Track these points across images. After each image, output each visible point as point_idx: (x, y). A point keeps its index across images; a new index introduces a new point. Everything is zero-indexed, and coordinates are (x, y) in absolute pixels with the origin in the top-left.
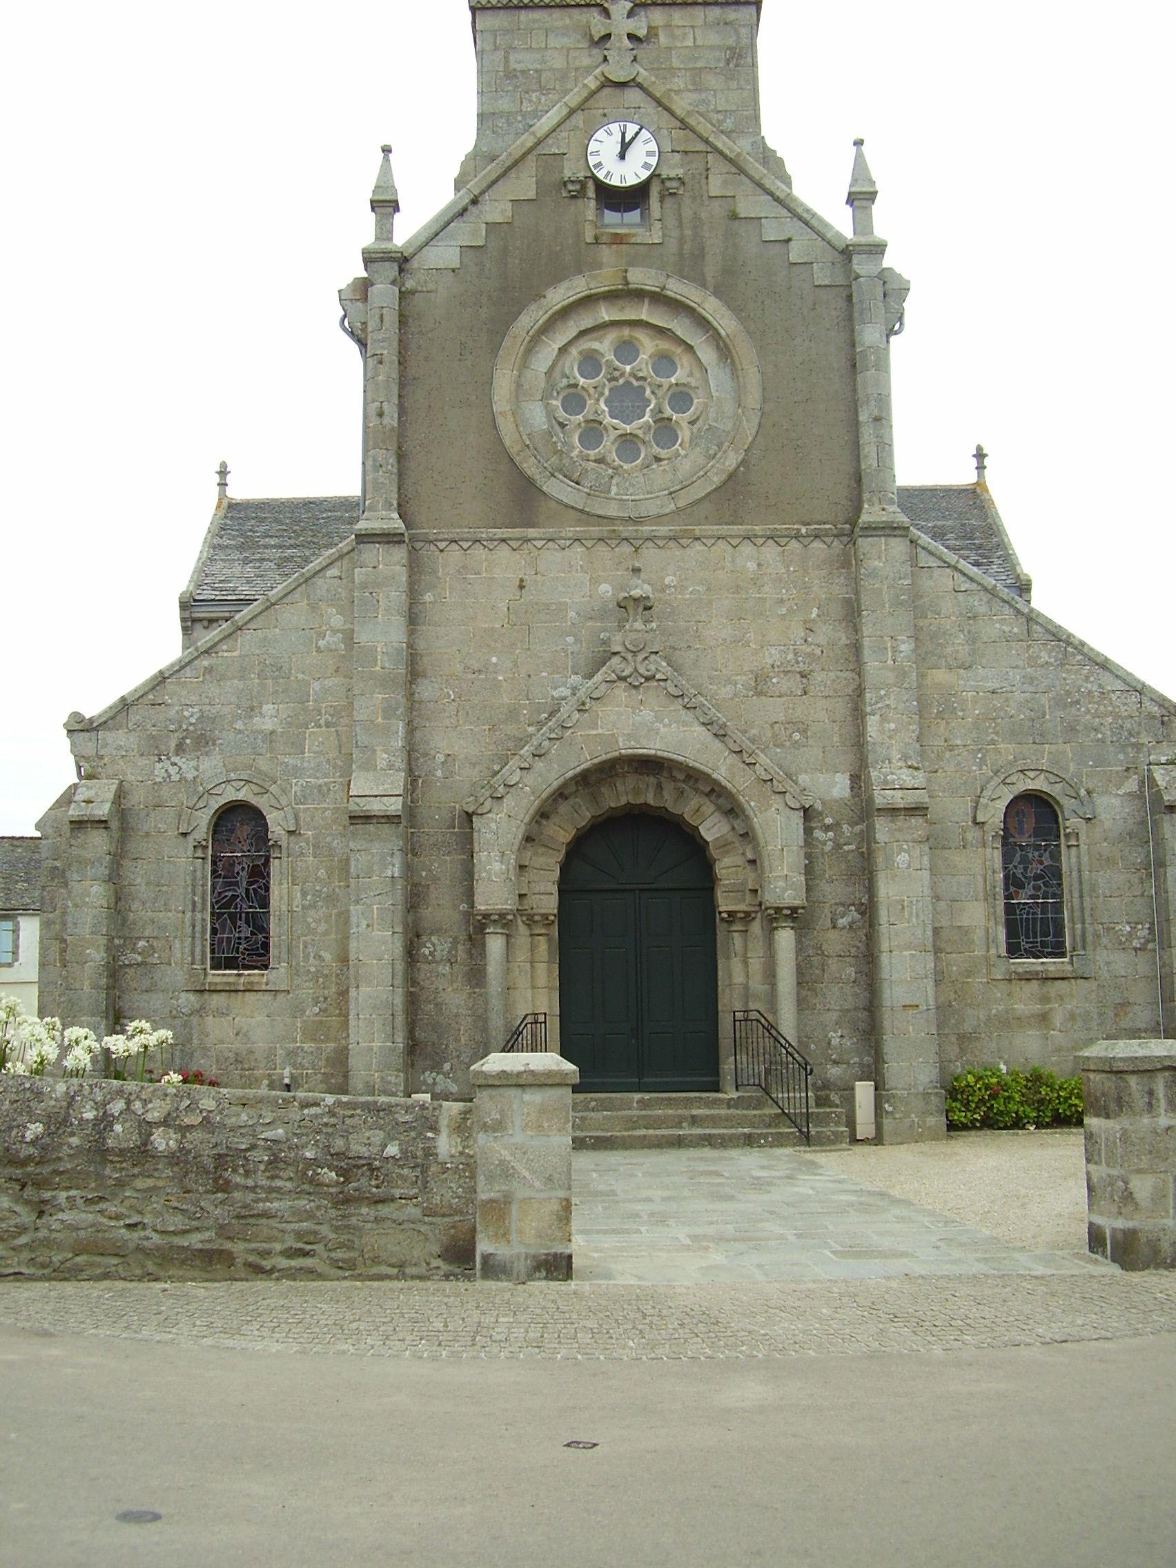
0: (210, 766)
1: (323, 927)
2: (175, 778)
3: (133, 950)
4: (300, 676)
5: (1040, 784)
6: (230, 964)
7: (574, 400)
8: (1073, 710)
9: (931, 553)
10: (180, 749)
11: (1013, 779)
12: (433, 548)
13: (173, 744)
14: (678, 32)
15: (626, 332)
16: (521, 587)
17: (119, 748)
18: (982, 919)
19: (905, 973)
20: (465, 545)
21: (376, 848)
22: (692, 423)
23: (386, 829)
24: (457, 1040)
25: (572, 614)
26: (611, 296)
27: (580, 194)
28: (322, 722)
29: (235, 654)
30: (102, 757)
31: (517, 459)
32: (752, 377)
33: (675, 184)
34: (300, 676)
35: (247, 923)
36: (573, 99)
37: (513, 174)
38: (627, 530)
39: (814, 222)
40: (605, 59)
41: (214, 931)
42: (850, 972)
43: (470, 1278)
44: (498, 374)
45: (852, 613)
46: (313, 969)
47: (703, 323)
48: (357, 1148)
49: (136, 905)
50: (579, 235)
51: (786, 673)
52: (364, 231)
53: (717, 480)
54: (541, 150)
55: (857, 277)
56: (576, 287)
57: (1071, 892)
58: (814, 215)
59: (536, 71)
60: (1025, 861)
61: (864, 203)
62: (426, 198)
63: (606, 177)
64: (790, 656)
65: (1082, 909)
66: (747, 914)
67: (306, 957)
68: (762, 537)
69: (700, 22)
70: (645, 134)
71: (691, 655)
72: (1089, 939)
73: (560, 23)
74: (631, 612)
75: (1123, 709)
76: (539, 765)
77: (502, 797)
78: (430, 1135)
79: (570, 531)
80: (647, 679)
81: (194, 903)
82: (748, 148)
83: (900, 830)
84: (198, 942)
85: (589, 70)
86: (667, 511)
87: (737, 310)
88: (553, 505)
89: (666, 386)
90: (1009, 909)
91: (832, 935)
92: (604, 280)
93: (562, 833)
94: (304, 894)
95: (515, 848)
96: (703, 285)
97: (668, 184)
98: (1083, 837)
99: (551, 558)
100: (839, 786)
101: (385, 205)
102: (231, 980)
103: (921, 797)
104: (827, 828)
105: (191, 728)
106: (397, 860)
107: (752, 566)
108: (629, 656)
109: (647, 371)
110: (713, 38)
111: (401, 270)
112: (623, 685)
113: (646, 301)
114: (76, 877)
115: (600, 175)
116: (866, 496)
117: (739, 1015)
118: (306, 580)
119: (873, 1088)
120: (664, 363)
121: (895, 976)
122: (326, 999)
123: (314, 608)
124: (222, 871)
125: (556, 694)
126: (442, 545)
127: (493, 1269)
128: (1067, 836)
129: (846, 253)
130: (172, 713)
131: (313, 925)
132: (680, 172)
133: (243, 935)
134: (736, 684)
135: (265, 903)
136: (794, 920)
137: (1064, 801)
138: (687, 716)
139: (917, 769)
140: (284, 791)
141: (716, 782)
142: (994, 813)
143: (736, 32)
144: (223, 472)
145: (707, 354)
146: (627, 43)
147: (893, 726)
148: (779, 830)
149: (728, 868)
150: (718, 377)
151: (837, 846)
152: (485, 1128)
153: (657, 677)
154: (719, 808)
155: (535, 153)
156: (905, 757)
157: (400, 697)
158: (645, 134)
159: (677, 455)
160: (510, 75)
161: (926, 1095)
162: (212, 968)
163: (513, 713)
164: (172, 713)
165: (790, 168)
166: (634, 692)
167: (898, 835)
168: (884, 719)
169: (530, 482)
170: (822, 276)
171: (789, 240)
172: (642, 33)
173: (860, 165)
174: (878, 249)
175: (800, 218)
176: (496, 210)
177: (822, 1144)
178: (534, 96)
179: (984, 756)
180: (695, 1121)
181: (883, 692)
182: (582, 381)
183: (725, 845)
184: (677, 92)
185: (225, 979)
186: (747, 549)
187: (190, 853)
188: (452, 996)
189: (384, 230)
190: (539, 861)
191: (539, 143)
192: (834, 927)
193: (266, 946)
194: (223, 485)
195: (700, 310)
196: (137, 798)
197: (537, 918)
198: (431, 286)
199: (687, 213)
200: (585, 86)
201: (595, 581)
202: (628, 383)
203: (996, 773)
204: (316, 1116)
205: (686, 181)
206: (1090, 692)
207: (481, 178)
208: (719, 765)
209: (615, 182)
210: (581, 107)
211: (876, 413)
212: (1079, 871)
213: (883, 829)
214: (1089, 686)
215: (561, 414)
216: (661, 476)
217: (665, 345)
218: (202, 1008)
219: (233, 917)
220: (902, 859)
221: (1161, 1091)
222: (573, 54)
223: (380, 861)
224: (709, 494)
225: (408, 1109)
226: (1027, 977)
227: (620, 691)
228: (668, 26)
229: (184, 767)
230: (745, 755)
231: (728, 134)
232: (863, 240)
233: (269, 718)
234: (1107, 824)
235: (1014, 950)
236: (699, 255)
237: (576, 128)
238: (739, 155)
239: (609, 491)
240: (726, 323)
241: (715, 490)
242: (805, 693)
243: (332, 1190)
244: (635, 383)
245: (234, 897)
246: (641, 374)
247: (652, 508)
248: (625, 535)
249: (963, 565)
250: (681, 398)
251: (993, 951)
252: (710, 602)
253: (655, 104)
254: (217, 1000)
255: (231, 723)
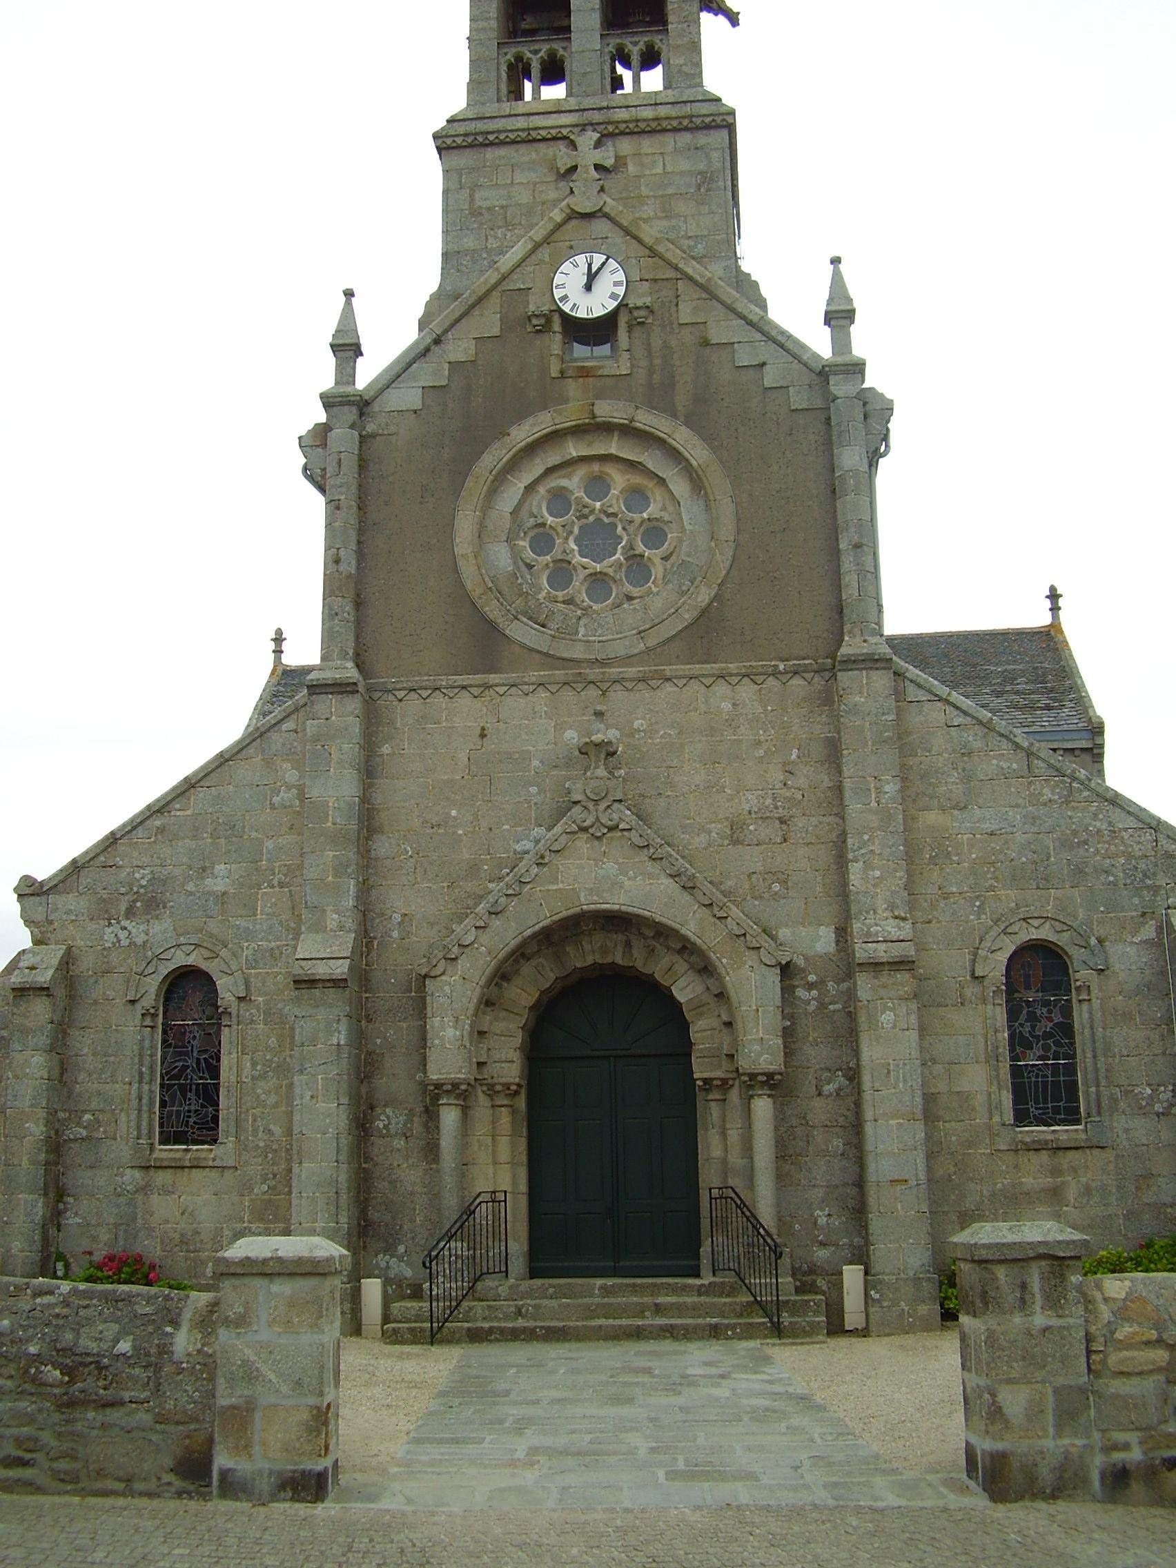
0: (160, 930)
1: (272, 1099)
2: (125, 942)
3: (79, 1124)
4: (254, 834)
5: (1045, 933)
6: (179, 1138)
7: (543, 540)
8: (1081, 851)
9: (920, 686)
10: (130, 913)
11: (1015, 928)
12: (391, 697)
13: (123, 907)
14: (647, 160)
15: (596, 467)
16: (483, 736)
17: (69, 912)
18: (983, 1084)
19: (893, 1145)
20: (425, 693)
21: (322, 1014)
22: (666, 559)
23: (332, 993)
24: (412, 1220)
25: (535, 763)
26: (578, 431)
27: (545, 329)
28: (275, 882)
29: (189, 812)
30: (51, 922)
31: (479, 603)
32: (726, 510)
33: (642, 313)
34: (254, 834)
35: (197, 1095)
36: (538, 233)
37: (476, 312)
38: (593, 673)
39: (789, 345)
40: (572, 192)
41: (163, 1104)
42: (838, 1143)
43: (205, 1497)
44: (460, 515)
45: (833, 753)
46: (262, 1144)
47: (674, 455)
48: (88, 1344)
49: (82, 1077)
50: (545, 370)
51: (764, 819)
52: (326, 377)
53: (688, 617)
54: (506, 286)
55: (835, 399)
56: (543, 423)
57: (1083, 1051)
58: (790, 337)
59: (502, 207)
60: (1032, 1017)
61: (842, 322)
62: (388, 338)
63: (572, 310)
64: (769, 801)
65: (1096, 1070)
66: (724, 1081)
67: (255, 1130)
68: (737, 675)
69: (670, 148)
70: (612, 264)
71: (662, 803)
72: (1105, 1102)
73: (526, 159)
74: (593, 759)
75: (1137, 848)
76: (496, 923)
77: (456, 959)
78: (169, 1329)
79: (534, 675)
80: (611, 829)
81: (141, 1074)
82: (720, 273)
83: (884, 986)
84: (145, 1115)
85: (555, 203)
86: (636, 651)
87: (709, 438)
88: (517, 649)
89: (638, 522)
90: (1016, 1072)
91: (818, 1103)
92: (571, 415)
93: (524, 994)
94: (254, 1065)
95: (470, 1012)
96: (674, 415)
97: (636, 314)
98: (1095, 991)
99: (514, 704)
100: (823, 941)
101: (347, 348)
102: (178, 1155)
103: (908, 950)
104: (811, 986)
105: (142, 891)
106: (343, 1027)
107: (726, 706)
108: (591, 805)
109: (619, 506)
110: (684, 165)
111: (361, 414)
112: (584, 836)
113: (616, 434)
114: (17, 1047)
115: (566, 308)
116: (847, 628)
117: (715, 1192)
118: (261, 735)
119: (862, 1274)
120: (636, 497)
121: (881, 1147)
122: (275, 1176)
123: (268, 763)
124: (174, 1040)
125: (518, 847)
126: (401, 694)
127: (231, 1487)
128: (1078, 989)
129: (823, 373)
130: (123, 875)
131: (263, 1097)
132: (648, 300)
133: (193, 1108)
134: (710, 832)
135: (215, 1072)
136: (773, 1087)
137: (1074, 952)
138: (651, 867)
139: (904, 919)
140: (234, 955)
141: (685, 939)
142: (995, 966)
143: (707, 156)
144: (279, 639)
145: (680, 487)
146: (594, 174)
147: (877, 873)
148: (753, 988)
149: (702, 1031)
150: (691, 512)
151: (822, 1006)
152: (227, 1322)
153: (621, 826)
154: (692, 967)
155: (499, 289)
156: (892, 907)
157: (351, 854)
158: (612, 264)
159: (650, 592)
160: (475, 212)
161: (917, 1280)
162: (161, 1143)
163: (473, 869)
164: (123, 875)
165: (764, 291)
166: (596, 843)
167: (883, 993)
168: (868, 866)
169: (492, 625)
170: (798, 399)
171: (764, 364)
172: (609, 163)
173: (837, 284)
174: (858, 368)
175: (775, 341)
176: (459, 349)
177: (796, 1336)
178: (499, 233)
179: (983, 903)
180: (658, 1309)
181: (866, 837)
182: (550, 520)
183: (699, 1007)
184: (645, 220)
185: (171, 1155)
186: (721, 688)
187: (138, 1022)
188: (403, 1171)
189: (345, 371)
190: (500, 1026)
191: (504, 278)
192: (820, 1095)
193: (216, 1119)
194: (278, 652)
195: (670, 440)
196: (86, 964)
197: (498, 1088)
198: (392, 429)
199: (657, 342)
200: (551, 218)
201: (560, 728)
202: (598, 520)
203: (996, 922)
204: (49, 1306)
205: (656, 308)
206: (1099, 831)
207: (443, 318)
208: (690, 921)
209: (581, 314)
210: (547, 240)
211: (856, 539)
212: (1092, 1028)
213: (865, 985)
214: (1098, 824)
215: (529, 555)
216: (631, 616)
217: (637, 479)
218: (148, 1185)
219: (184, 1089)
220: (887, 1018)
221: (1035, 1284)
222: (540, 188)
223: (326, 1029)
224: (681, 631)
225: (150, 1300)
226: (1037, 1147)
227: (582, 844)
228: (637, 155)
229: (134, 931)
230: (716, 909)
231: (699, 259)
232: (839, 360)
233: (221, 879)
234: (1122, 976)
235: (1021, 1117)
236: (670, 385)
237: (542, 261)
238: (709, 279)
239: (577, 633)
240: (697, 452)
241: (686, 627)
242: (785, 841)
243: (57, 1391)
244: (606, 520)
245: (185, 1068)
246: (611, 510)
247: (620, 649)
248: (591, 678)
249: (955, 697)
250: (654, 533)
251: (996, 1119)
252: (682, 745)
253: (622, 233)
254: (163, 1177)
255: (183, 884)
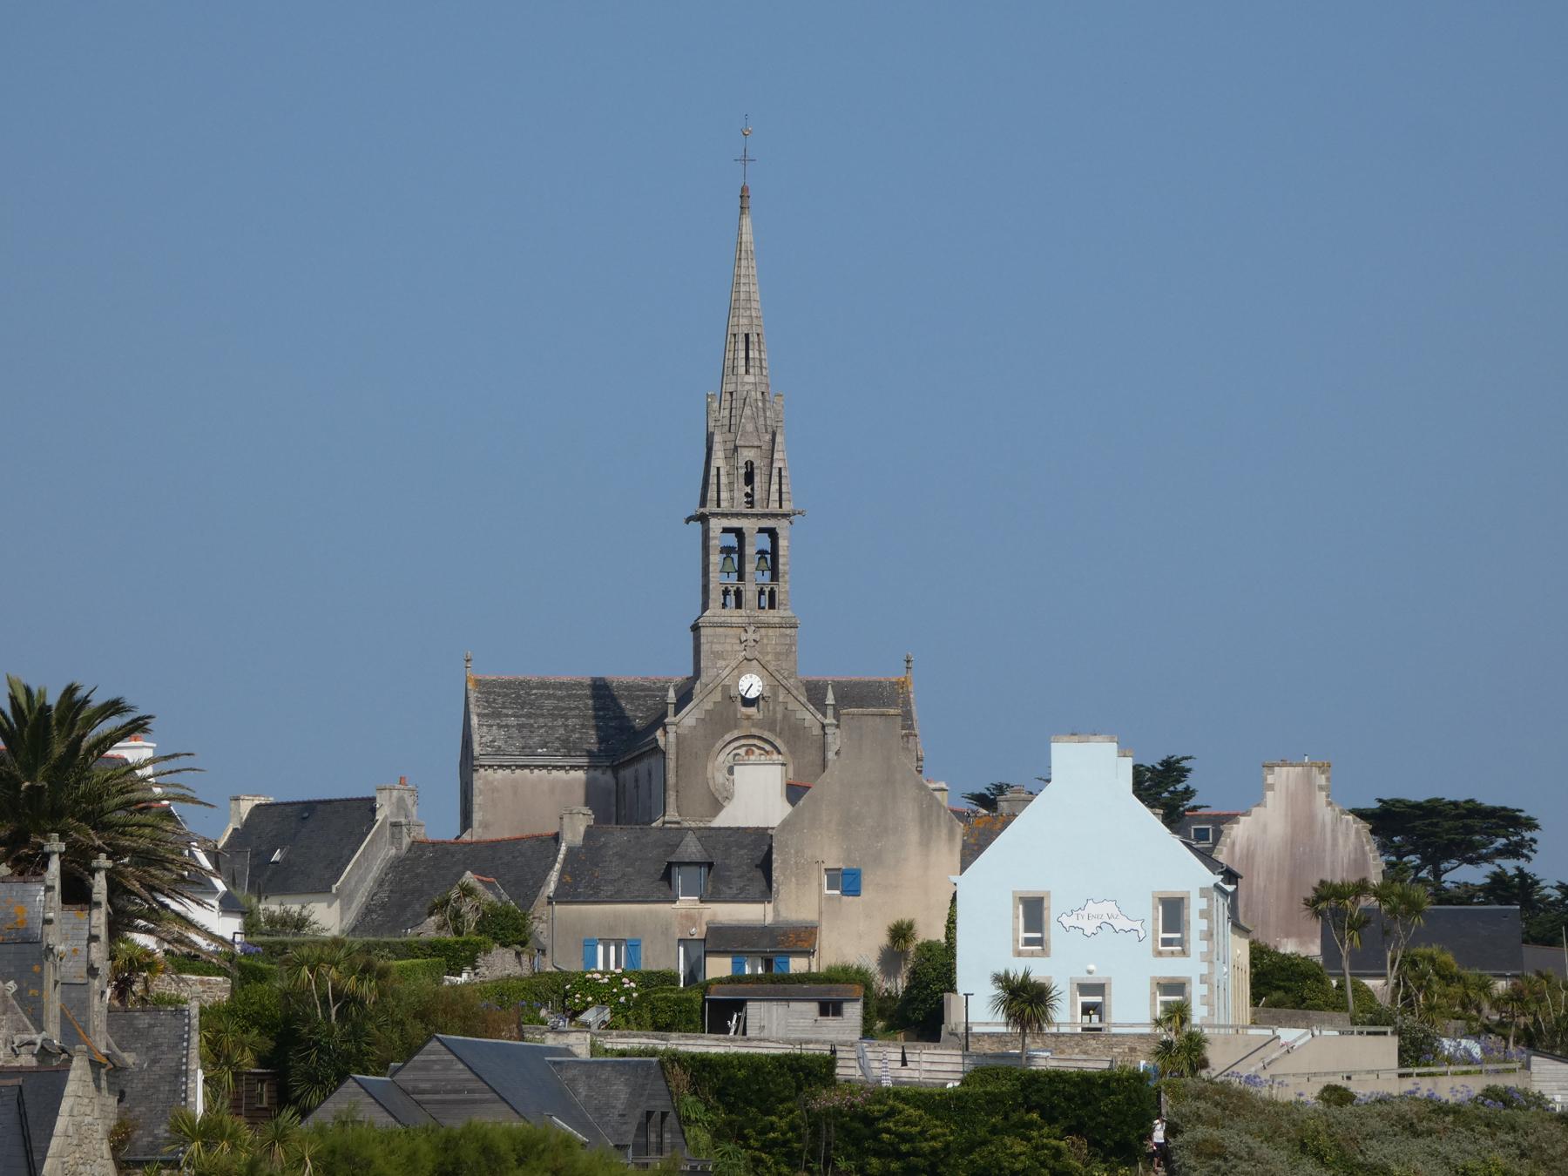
36: (734, 664)
56: (736, 734)
